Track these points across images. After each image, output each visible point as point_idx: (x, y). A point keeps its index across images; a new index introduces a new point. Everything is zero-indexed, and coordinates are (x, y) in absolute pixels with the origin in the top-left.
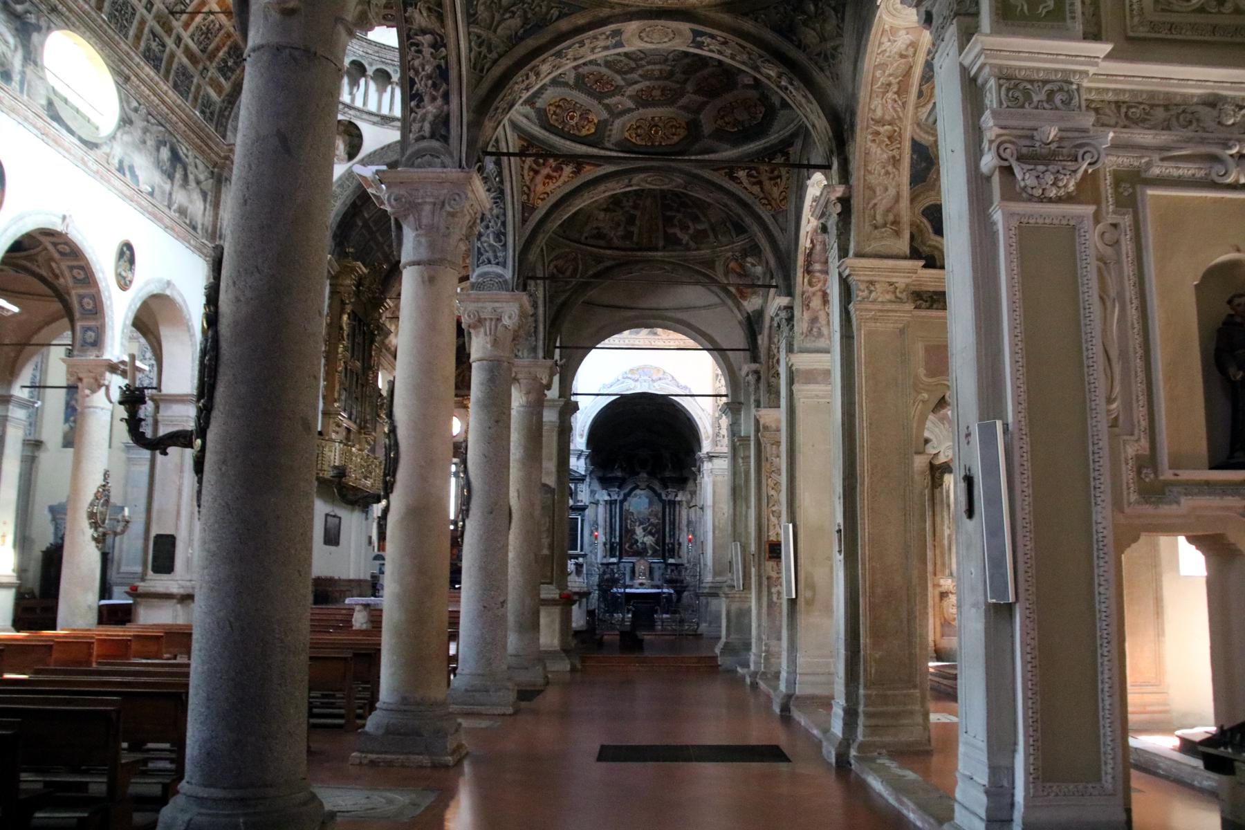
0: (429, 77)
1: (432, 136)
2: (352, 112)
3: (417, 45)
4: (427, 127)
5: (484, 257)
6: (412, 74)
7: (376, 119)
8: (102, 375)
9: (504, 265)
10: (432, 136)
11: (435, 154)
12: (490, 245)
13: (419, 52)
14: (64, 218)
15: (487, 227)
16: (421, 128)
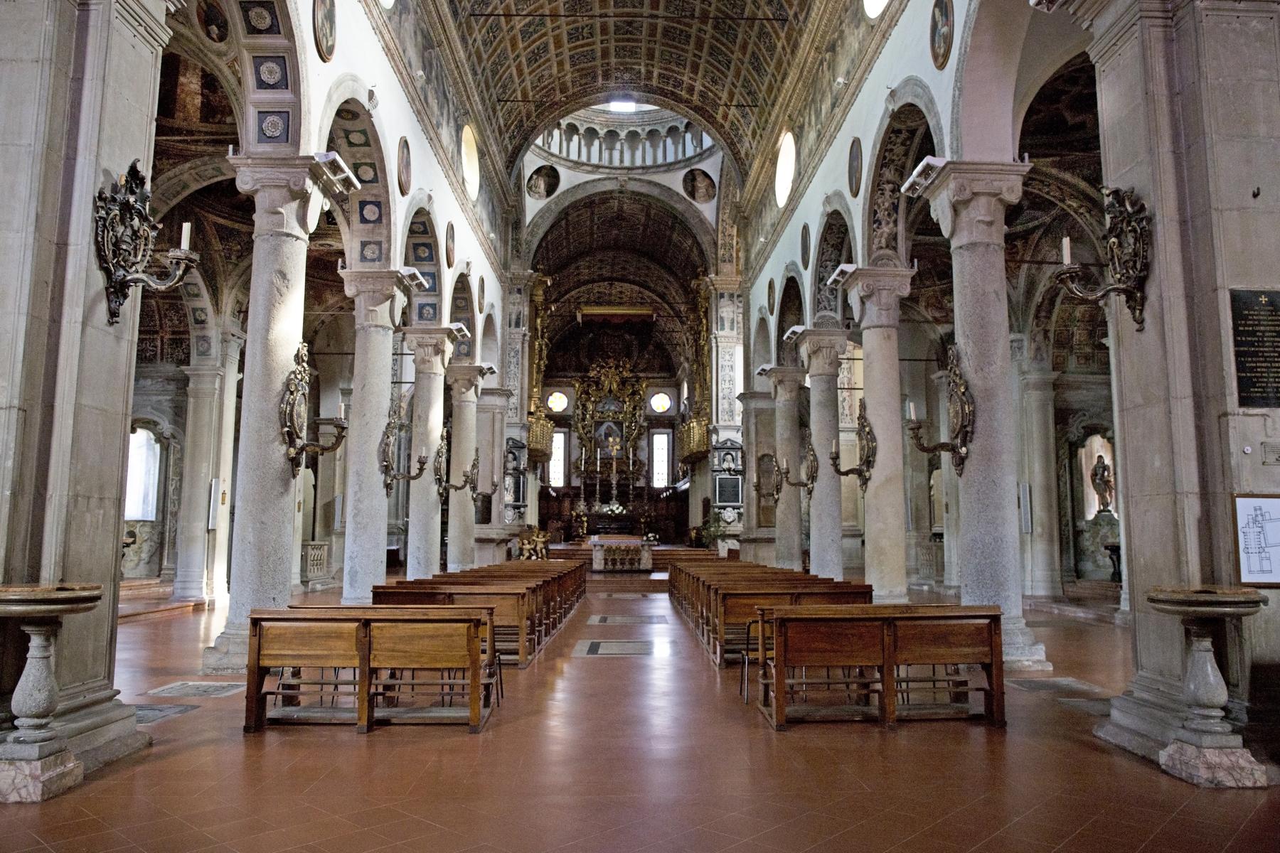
1: (887, 247)
4: (883, 241)
8: (475, 378)
10: (887, 247)
11: (889, 258)
14: (468, 264)
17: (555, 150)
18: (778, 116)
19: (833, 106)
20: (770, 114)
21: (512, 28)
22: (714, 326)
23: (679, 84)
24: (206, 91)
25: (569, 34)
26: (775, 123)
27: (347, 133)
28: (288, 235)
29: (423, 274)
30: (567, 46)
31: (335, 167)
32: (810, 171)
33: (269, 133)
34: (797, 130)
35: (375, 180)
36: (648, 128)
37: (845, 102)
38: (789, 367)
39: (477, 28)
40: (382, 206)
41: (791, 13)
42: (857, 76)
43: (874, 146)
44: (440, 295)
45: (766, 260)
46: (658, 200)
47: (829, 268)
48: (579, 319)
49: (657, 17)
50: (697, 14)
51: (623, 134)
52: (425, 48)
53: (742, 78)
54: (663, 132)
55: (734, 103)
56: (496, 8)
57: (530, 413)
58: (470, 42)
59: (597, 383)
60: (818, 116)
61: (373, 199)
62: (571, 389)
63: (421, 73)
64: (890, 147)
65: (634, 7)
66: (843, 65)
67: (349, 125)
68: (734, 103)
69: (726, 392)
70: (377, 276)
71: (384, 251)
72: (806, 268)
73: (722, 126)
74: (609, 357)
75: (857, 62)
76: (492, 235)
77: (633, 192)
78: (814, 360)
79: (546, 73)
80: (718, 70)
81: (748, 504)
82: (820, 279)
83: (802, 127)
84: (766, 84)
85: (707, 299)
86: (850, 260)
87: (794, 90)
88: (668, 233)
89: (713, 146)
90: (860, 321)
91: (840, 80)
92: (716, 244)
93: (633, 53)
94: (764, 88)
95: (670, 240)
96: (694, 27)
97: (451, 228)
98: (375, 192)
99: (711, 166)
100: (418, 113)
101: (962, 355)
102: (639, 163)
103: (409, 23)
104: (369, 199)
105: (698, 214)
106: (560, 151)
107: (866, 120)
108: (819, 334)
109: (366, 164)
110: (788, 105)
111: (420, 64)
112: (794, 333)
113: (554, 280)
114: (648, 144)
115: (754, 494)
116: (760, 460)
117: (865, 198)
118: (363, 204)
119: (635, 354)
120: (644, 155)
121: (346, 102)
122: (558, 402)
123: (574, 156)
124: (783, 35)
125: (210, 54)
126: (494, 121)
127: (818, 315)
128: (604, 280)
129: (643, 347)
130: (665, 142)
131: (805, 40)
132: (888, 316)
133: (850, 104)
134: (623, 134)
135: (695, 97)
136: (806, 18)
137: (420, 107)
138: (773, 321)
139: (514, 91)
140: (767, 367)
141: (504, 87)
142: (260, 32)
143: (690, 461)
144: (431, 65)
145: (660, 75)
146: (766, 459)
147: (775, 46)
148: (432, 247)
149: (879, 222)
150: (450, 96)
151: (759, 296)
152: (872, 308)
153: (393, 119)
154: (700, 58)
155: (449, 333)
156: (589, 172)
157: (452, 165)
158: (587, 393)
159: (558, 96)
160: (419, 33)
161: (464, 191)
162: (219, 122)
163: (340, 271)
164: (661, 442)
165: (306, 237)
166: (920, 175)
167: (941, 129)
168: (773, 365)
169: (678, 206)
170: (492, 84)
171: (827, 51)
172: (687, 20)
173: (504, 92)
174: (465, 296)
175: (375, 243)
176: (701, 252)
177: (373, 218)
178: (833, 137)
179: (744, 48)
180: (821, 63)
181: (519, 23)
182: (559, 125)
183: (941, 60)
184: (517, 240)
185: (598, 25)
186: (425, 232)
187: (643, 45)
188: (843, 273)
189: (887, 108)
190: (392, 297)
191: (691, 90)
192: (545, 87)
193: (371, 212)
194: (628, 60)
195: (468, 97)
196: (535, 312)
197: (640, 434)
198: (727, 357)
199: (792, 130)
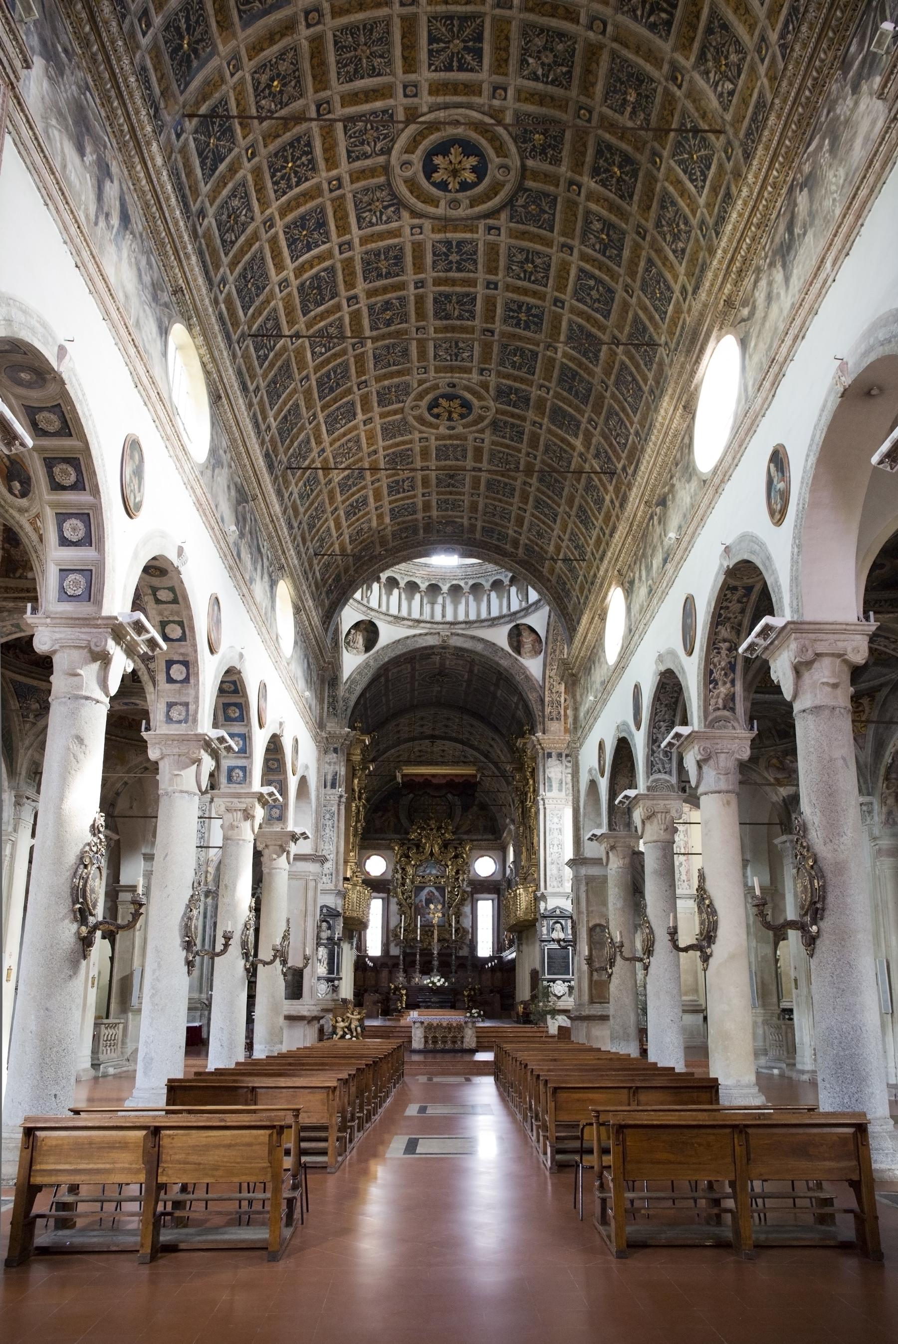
0: (723, 669)
2: (373, 613)
4: (720, 701)
6: (712, 667)
7: (410, 623)
9: (670, 773)
10: (725, 708)
11: (727, 720)
13: (719, 653)
14: (281, 724)
16: (717, 703)
17: (374, 604)
18: (607, 571)
19: (665, 561)
20: (598, 569)
21: (330, 481)
22: (541, 786)
23: (503, 537)
24: (7, 546)
25: (389, 487)
26: (604, 579)
27: (155, 590)
28: (87, 698)
29: (232, 736)
30: (386, 499)
31: (139, 627)
32: (641, 627)
33: (70, 592)
34: (627, 585)
35: (183, 638)
36: (471, 582)
37: (677, 558)
38: (621, 832)
39: (293, 482)
40: (189, 665)
42: (690, 531)
43: (709, 603)
44: (250, 757)
45: (596, 719)
46: (482, 656)
47: (663, 729)
48: (399, 780)
49: (480, 470)
50: (521, 468)
51: (445, 588)
52: (239, 503)
53: (569, 531)
54: (487, 586)
55: (561, 557)
56: (313, 461)
57: (346, 879)
58: (286, 495)
59: (418, 846)
60: (649, 569)
61: (181, 658)
62: (389, 852)
63: (233, 528)
64: (725, 604)
65: (458, 460)
66: (674, 519)
67: (156, 582)
68: (561, 557)
69: (555, 856)
70: (183, 739)
71: (191, 712)
72: (638, 729)
73: (549, 580)
74: (430, 819)
75: (689, 516)
76: (307, 694)
77: (456, 648)
78: (648, 826)
80: (544, 523)
82: (653, 740)
83: (632, 583)
84: (594, 538)
85: (534, 759)
86: (685, 722)
88: (492, 689)
89: (539, 600)
90: (697, 787)
91: (672, 535)
92: (542, 701)
93: (456, 506)
94: (592, 542)
96: (519, 481)
97: (263, 688)
98: (182, 651)
99: (538, 620)
100: (231, 568)
101: (810, 826)
102: (461, 617)
103: (222, 477)
104: (176, 658)
105: (523, 670)
107: (699, 577)
109: (174, 622)
110: (617, 560)
111: (233, 519)
112: (626, 797)
113: (372, 739)
114: (471, 598)
118: (170, 664)
119: (458, 811)
120: (467, 609)
121: (154, 559)
122: (376, 866)
123: (394, 611)
124: (611, 488)
125: (11, 511)
126: (310, 576)
127: (652, 778)
128: (427, 737)
129: (466, 808)
130: (489, 595)
131: (634, 495)
132: (727, 780)
133: (683, 559)
134: (445, 588)
135: (521, 551)
136: (635, 471)
137: (232, 562)
138: (603, 784)
139: (332, 544)
140: (598, 832)
141: (322, 540)
142: (64, 488)
143: (517, 930)
144: (244, 519)
145: (483, 527)
148: (243, 708)
149: (715, 682)
150: (264, 551)
151: (589, 757)
152: (710, 773)
153: (204, 576)
154: (525, 511)
155: (260, 797)
156: (410, 627)
157: (264, 621)
158: (408, 857)
159: (378, 549)
160: (232, 487)
161: (277, 648)
162: (20, 578)
163: (144, 734)
165: (107, 700)
166: (758, 635)
167: (779, 587)
168: (604, 829)
169: (502, 662)
170: (309, 538)
171: (657, 505)
172: (512, 474)
173: (321, 546)
174: (279, 757)
175: (181, 704)
177: (180, 678)
178: (665, 593)
179: (570, 502)
180: (651, 518)
181: (337, 477)
182: (378, 579)
183: (777, 516)
184: (334, 697)
185: (420, 477)
186: (236, 691)
187: (466, 498)
188: (678, 736)
189: (721, 565)
190: (198, 761)
191: (516, 543)
192: (364, 540)
193: (177, 672)
194: (450, 513)
195: (284, 552)
196: (352, 772)
198: (556, 820)
199: (622, 585)
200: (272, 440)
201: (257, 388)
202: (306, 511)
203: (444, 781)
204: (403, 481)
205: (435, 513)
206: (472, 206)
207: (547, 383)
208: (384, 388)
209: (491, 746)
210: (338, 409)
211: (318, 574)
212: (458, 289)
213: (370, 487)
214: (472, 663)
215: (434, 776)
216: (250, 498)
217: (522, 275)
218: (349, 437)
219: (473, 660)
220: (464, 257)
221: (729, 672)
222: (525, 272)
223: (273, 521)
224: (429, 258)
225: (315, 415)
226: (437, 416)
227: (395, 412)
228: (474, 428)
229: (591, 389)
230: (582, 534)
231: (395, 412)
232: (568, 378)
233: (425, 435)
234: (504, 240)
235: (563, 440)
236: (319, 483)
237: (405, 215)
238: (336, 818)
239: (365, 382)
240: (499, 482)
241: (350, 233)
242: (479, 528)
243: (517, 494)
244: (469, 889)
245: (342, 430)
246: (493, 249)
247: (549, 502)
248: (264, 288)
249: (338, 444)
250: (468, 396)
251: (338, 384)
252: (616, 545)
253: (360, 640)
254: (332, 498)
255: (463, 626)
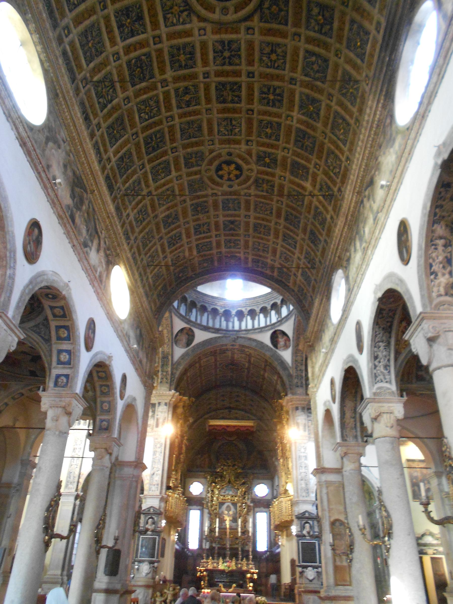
0: (441, 263)
3: (435, 245)
5: (378, 379)
6: (431, 261)
9: (390, 382)
10: (446, 294)
12: (381, 372)
13: (436, 249)
15: (380, 362)
16: (438, 291)
17: (193, 319)
21: (156, 216)
23: (265, 265)
36: (249, 309)
39: (130, 207)
41: (336, 189)
46: (255, 350)
54: (258, 310)
58: (125, 214)
64: (440, 202)
65: (235, 210)
74: (228, 459)
79: (181, 254)
80: (289, 251)
81: (326, 563)
84: (320, 250)
87: (341, 235)
88: (262, 373)
94: (319, 254)
95: (264, 379)
99: (288, 328)
106: (196, 320)
108: (379, 402)
114: (249, 318)
115: (329, 553)
116: (333, 524)
117: (419, 257)
124: (330, 208)
126: (145, 278)
128: (226, 408)
135: (275, 274)
141: (152, 257)
145: (253, 259)
146: (337, 524)
147: (326, 219)
156: (213, 332)
164: (262, 518)
176: (282, 381)
186: (64, 316)
197: (248, 511)
198: (303, 450)
200: (112, 169)
201: (99, 126)
202: (141, 232)
203: (234, 430)
204: (203, 225)
205: (224, 250)
206: (236, 12)
207: (287, 146)
208: (188, 154)
209: (263, 413)
210: (159, 164)
211: (150, 280)
212: (230, 79)
213: (183, 227)
214: (250, 356)
215: (228, 426)
216: (89, 192)
217: (269, 64)
218: (167, 187)
219: (250, 354)
220: (233, 53)
221: (446, 265)
222: (271, 61)
223: (108, 217)
224: (211, 56)
225: (143, 166)
226: (221, 177)
227: (196, 173)
228: (244, 186)
229: (315, 141)
230: (313, 250)
231: (196, 173)
232: (302, 138)
233: (215, 191)
234: (257, 38)
235: (299, 185)
236: (149, 216)
237: (195, 19)
238: (163, 447)
239: (175, 148)
240: (261, 225)
241: (159, 29)
242: (250, 259)
243: (272, 232)
244: (252, 505)
245: (163, 181)
246: (250, 45)
247: (291, 234)
248: (101, 53)
249: (160, 191)
250: (240, 162)
251: (158, 146)
252: (336, 238)
253: (184, 339)
254: (158, 229)
255: (244, 332)
